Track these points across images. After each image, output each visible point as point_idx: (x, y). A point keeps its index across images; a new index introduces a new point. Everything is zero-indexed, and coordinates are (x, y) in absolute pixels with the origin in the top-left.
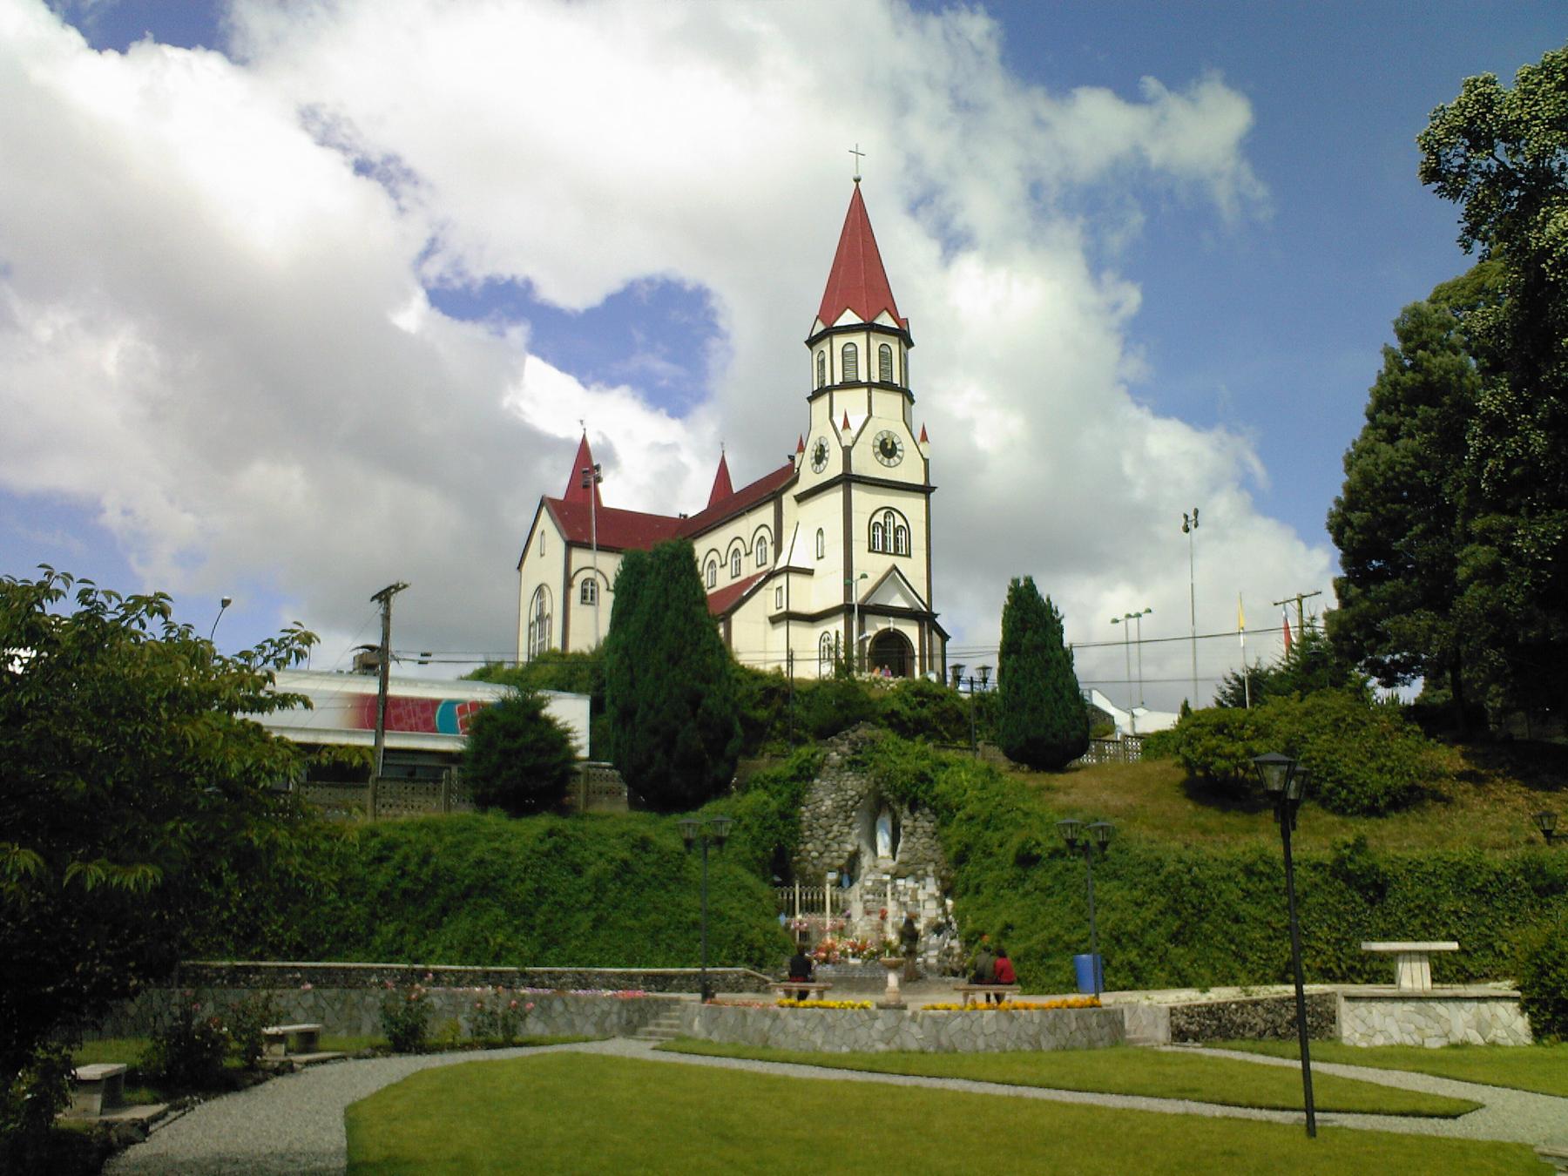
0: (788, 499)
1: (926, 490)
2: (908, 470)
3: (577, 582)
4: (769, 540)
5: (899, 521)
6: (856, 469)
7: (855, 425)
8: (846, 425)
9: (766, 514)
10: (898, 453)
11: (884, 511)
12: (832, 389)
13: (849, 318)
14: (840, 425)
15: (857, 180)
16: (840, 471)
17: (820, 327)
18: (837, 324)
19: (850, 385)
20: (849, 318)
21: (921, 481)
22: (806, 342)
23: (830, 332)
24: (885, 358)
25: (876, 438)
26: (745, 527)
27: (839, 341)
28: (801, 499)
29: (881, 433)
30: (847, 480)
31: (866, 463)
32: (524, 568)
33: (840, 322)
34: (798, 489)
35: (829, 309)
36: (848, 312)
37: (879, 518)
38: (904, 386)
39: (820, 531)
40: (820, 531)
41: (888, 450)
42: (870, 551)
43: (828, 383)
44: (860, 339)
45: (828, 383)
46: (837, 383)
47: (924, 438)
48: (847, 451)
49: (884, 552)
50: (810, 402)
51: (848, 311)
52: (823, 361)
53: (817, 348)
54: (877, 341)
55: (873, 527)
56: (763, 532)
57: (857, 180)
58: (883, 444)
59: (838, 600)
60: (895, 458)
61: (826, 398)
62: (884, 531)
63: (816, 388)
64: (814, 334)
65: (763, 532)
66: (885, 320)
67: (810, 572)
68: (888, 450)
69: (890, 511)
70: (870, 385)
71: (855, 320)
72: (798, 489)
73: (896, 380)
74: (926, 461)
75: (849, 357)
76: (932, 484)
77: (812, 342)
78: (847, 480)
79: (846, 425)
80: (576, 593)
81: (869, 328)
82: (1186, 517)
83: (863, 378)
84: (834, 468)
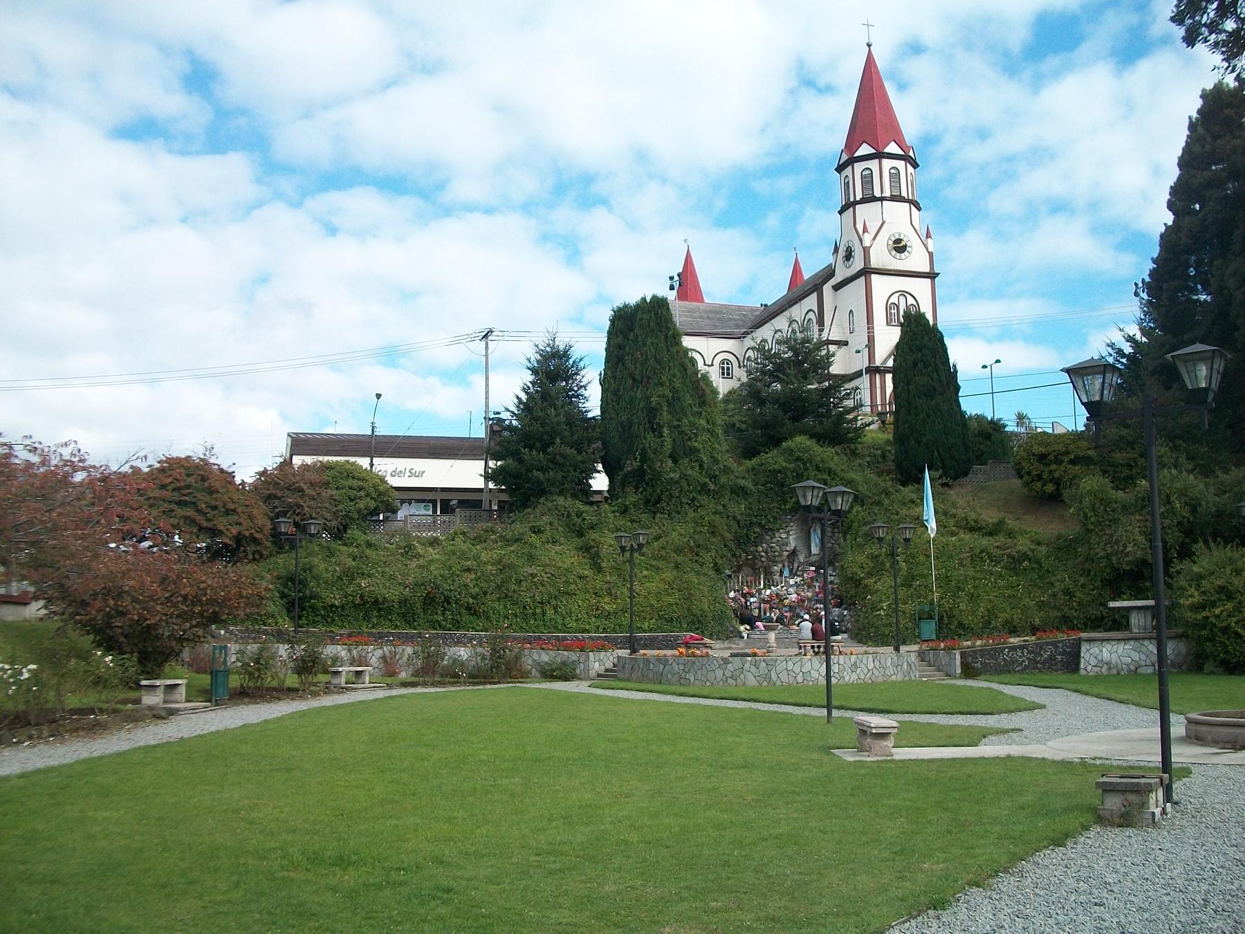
0: (827, 289)
1: (932, 276)
2: (916, 260)
4: (815, 321)
5: (911, 301)
6: (874, 263)
7: (872, 230)
8: (865, 230)
9: (811, 302)
10: (908, 249)
13: (865, 150)
14: (861, 232)
15: (869, 45)
16: (862, 266)
17: (845, 157)
18: (855, 155)
19: (869, 199)
20: (865, 150)
22: (836, 170)
23: (852, 161)
24: (895, 176)
25: (889, 239)
26: (797, 312)
27: (859, 167)
28: (836, 288)
29: (894, 235)
30: (867, 272)
34: (833, 281)
35: (851, 144)
36: (865, 145)
37: (894, 299)
38: (910, 198)
39: (851, 311)
40: (851, 311)
41: (899, 247)
42: (888, 324)
43: (852, 199)
44: (873, 164)
45: (852, 199)
46: (858, 199)
47: (928, 236)
48: (866, 251)
50: (840, 214)
51: (865, 144)
52: (848, 182)
53: (844, 173)
54: (887, 164)
55: (888, 307)
56: (811, 315)
57: (869, 45)
58: (898, 241)
59: (861, 363)
60: (906, 253)
62: (898, 307)
63: (844, 203)
64: (841, 163)
65: (811, 315)
66: (892, 148)
67: (846, 343)
68: (899, 247)
69: (903, 293)
70: (882, 199)
71: (870, 151)
72: (833, 281)
73: (904, 194)
74: (931, 254)
75: (867, 180)
76: (936, 272)
77: (840, 169)
78: (867, 272)
79: (865, 230)
81: (879, 155)
82: (1136, 284)
83: (877, 194)
84: (858, 264)
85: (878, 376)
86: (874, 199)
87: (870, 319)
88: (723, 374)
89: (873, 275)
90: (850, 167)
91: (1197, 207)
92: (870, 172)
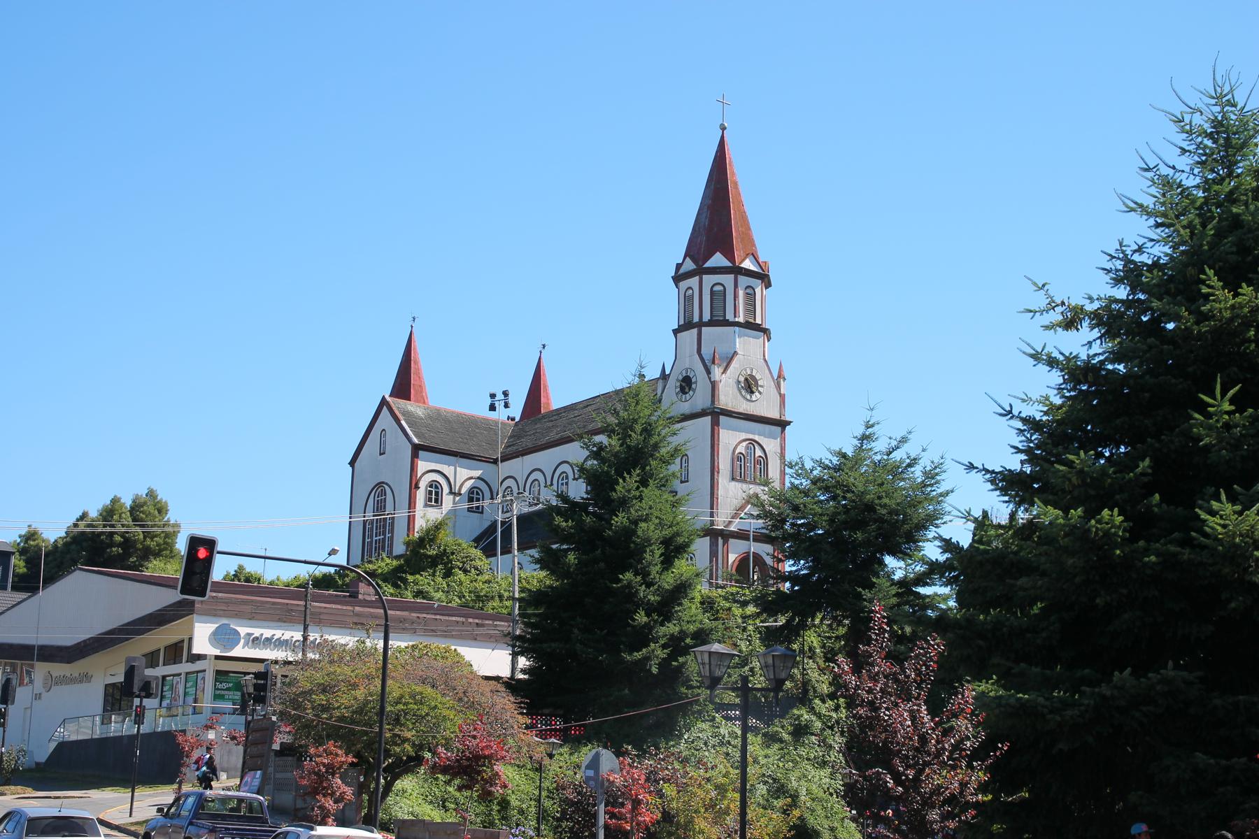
3: (423, 484)
11: (744, 444)
12: (701, 325)
13: (718, 260)
15: (723, 128)
17: (689, 265)
18: (705, 266)
21: (774, 414)
23: (700, 271)
27: (709, 280)
31: (729, 397)
32: (356, 465)
33: (708, 264)
41: (749, 385)
43: (696, 319)
44: (728, 279)
49: (744, 481)
61: (695, 331)
66: (748, 264)
71: (726, 263)
75: (718, 297)
76: (788, 418)
80: (421, 495)
83: (730, 317)
85: (720, 541)
86: (727, 323)
87: (714, 470)
88: (430, 500)
89: (720, 416)
90: (697, 278)
91: (1191, 445)
92: (721, 288)
